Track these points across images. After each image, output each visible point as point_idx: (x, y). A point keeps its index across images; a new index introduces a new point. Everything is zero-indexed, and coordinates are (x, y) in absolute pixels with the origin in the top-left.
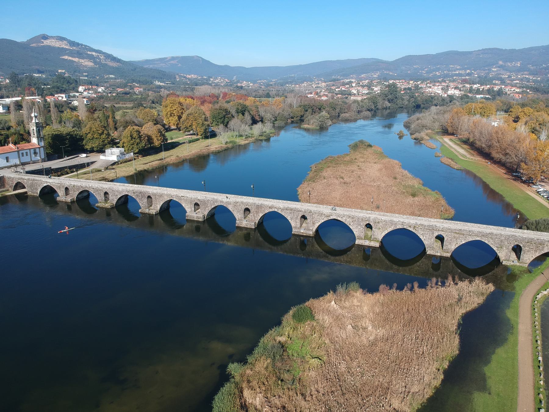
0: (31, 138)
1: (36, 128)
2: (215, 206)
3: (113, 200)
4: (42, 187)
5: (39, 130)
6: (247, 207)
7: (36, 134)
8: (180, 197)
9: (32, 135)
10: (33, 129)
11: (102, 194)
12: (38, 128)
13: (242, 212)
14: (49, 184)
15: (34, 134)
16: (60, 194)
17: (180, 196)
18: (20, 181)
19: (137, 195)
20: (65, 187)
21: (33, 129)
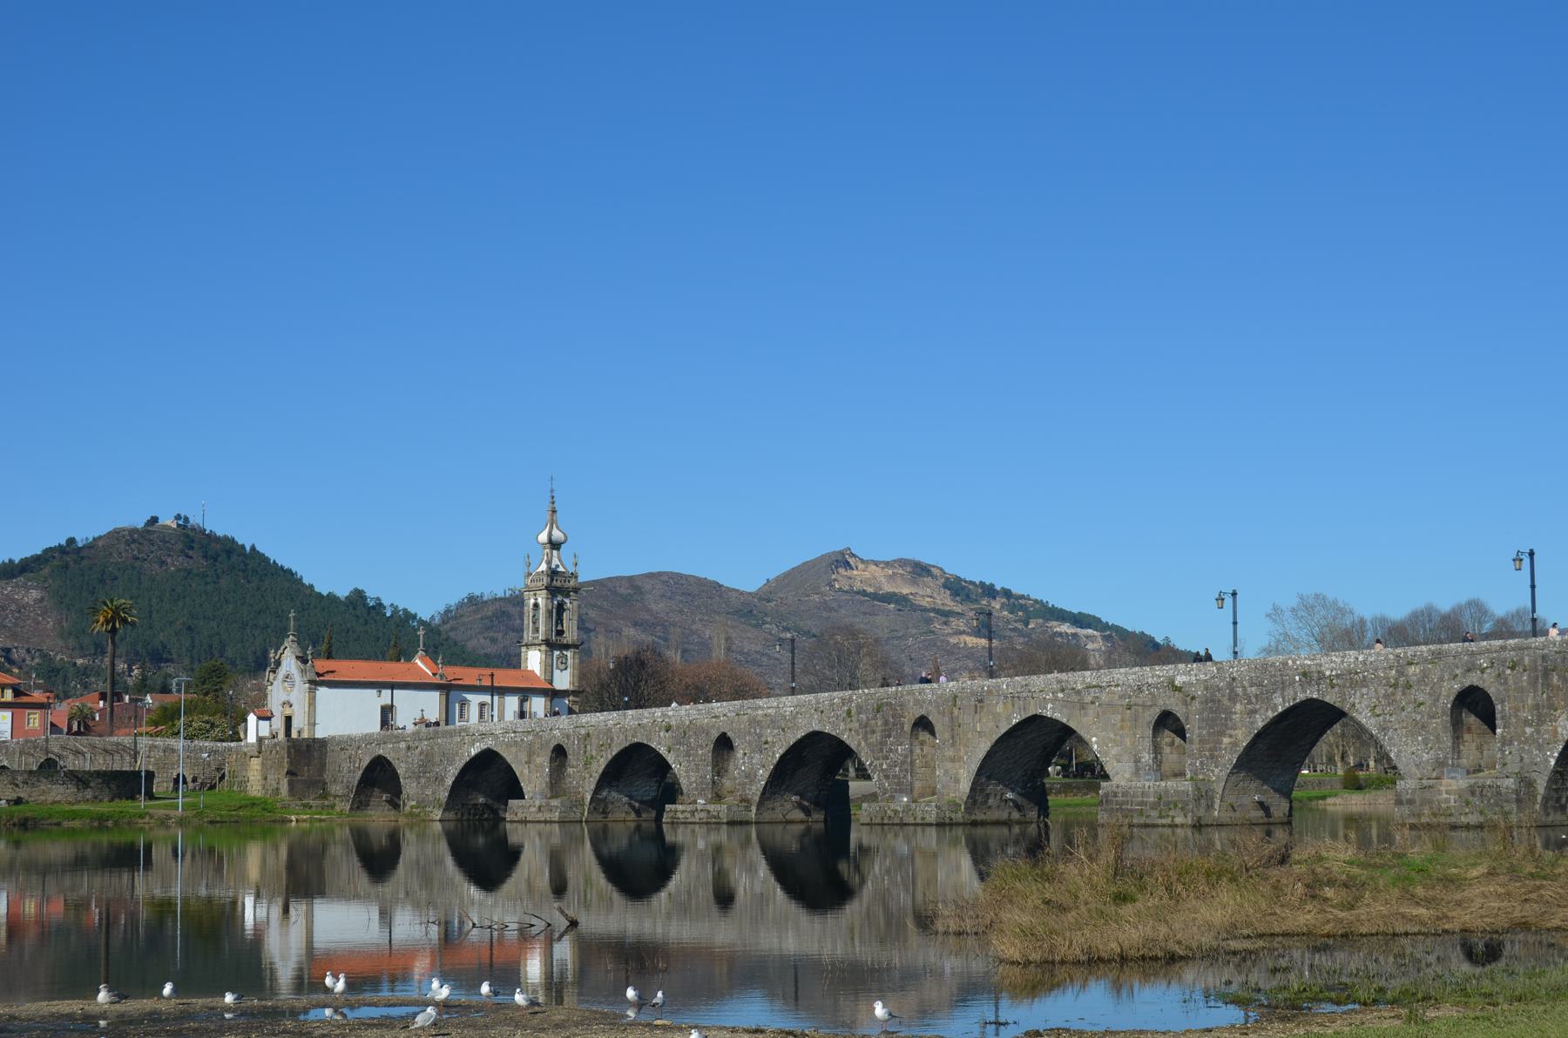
0: (523, 649)
2: (1271, 714)
3: (750, 776)
4: (463, 762)
6: (1474, 679)
7: (542, 628)
8: (1078, 692)
9: (528, 636)
10: (536, 605)
11: (705, 752)
13: (1440, 724)
14: (489, 743)
15: (537, 630)
16: (527, 788)
17: (1079, 687)
18: (381, 752)
19: (867, 730)
20: (552, 746)
21: (536, 605)
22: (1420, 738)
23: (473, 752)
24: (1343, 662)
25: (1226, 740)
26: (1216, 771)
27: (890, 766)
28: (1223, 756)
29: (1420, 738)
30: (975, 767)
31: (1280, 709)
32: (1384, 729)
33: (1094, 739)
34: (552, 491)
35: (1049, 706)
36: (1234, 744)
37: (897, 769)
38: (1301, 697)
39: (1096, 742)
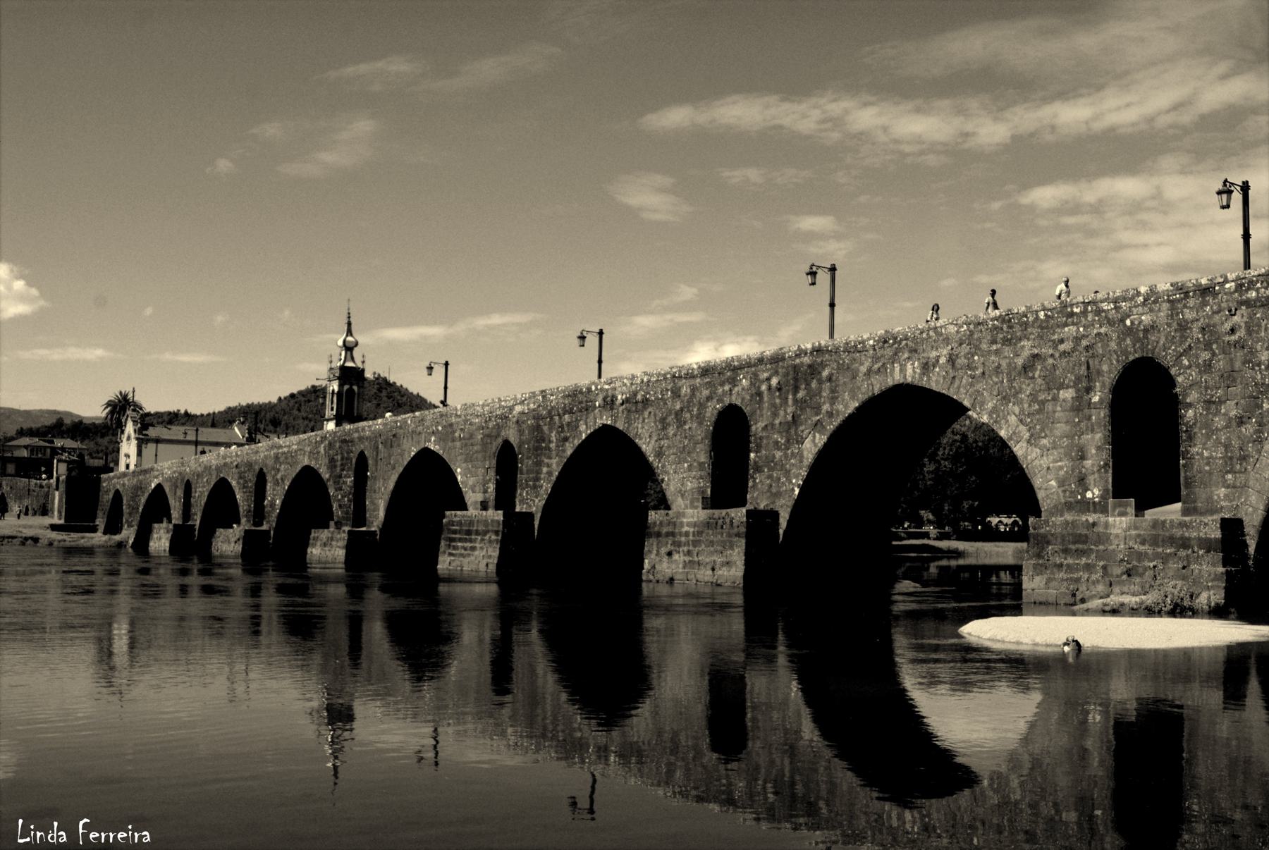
1: (341, 386)
2: (577, 442)
5: (350, 391)
10: (333, 391)
12: (346, 387)
15: (332, 409)
21: (333, 391)
22: (686, 465)
23: (153, 486)
24: (632, 384)
25: (545, 470)
26: (537, 501)
27: (343, 497)
28: (541, 487)
29: (686, 465)
30: (387, 497)
31: (584, 436)
32: (659, 454)
33: (459, 470)
34: (349, 309)
35: (433, 438)
36: (550, 474)
37: (346, 499)
38: (599, 422)
39: (461, 474)
